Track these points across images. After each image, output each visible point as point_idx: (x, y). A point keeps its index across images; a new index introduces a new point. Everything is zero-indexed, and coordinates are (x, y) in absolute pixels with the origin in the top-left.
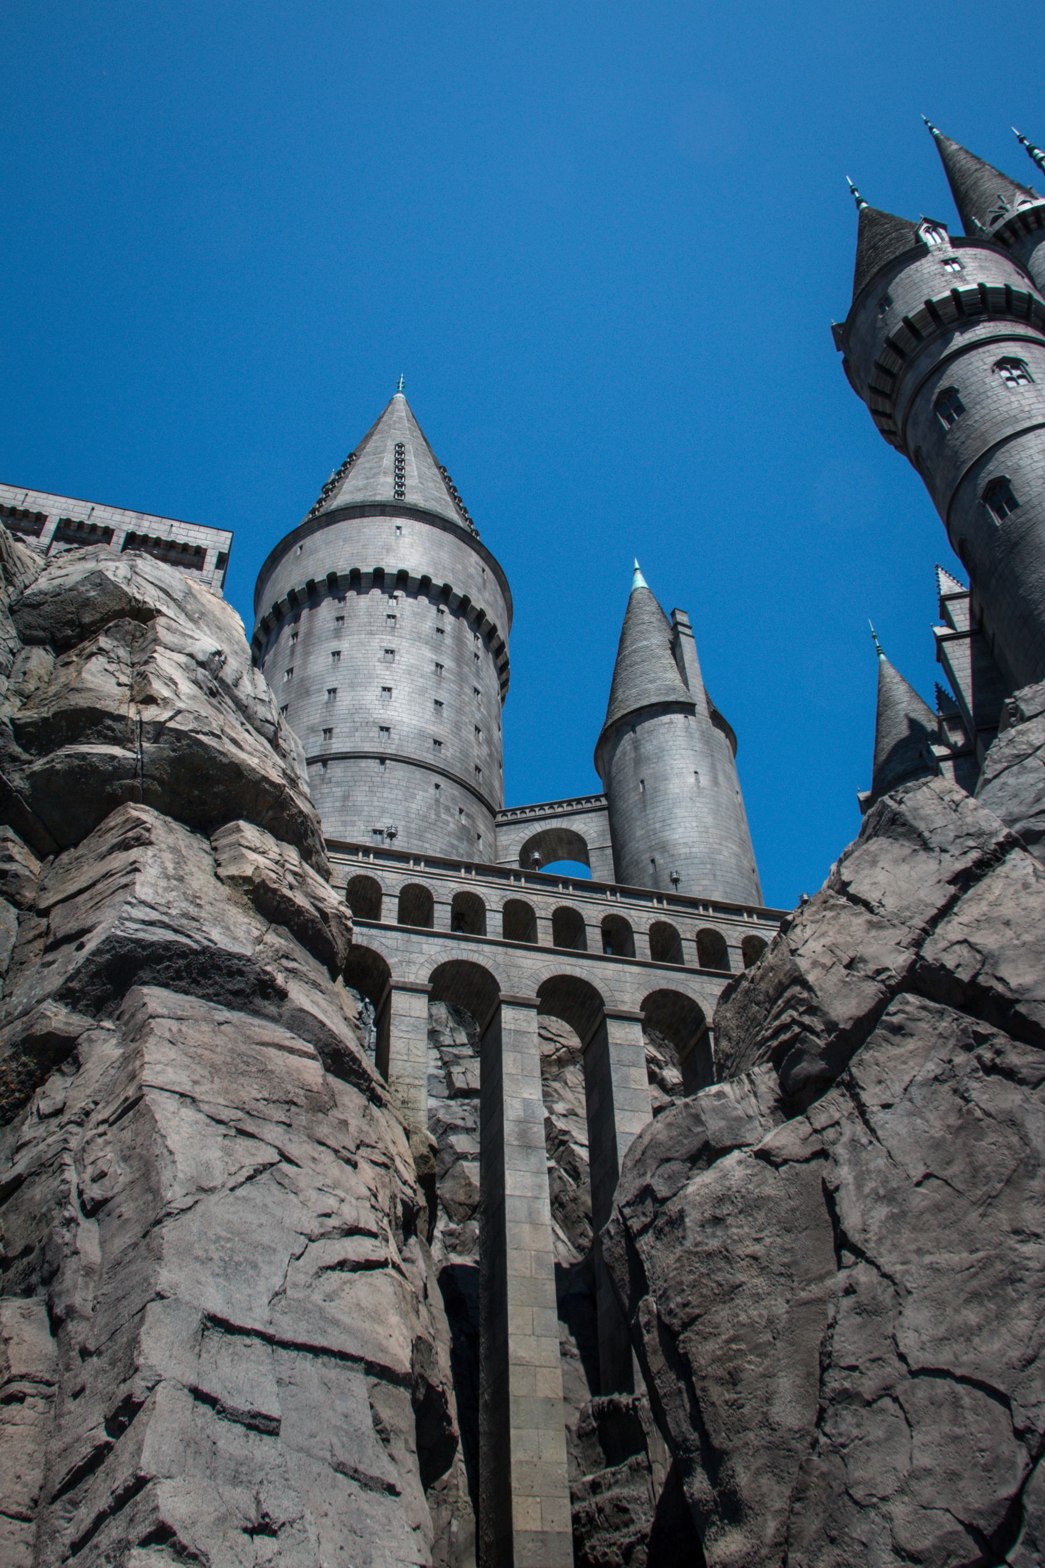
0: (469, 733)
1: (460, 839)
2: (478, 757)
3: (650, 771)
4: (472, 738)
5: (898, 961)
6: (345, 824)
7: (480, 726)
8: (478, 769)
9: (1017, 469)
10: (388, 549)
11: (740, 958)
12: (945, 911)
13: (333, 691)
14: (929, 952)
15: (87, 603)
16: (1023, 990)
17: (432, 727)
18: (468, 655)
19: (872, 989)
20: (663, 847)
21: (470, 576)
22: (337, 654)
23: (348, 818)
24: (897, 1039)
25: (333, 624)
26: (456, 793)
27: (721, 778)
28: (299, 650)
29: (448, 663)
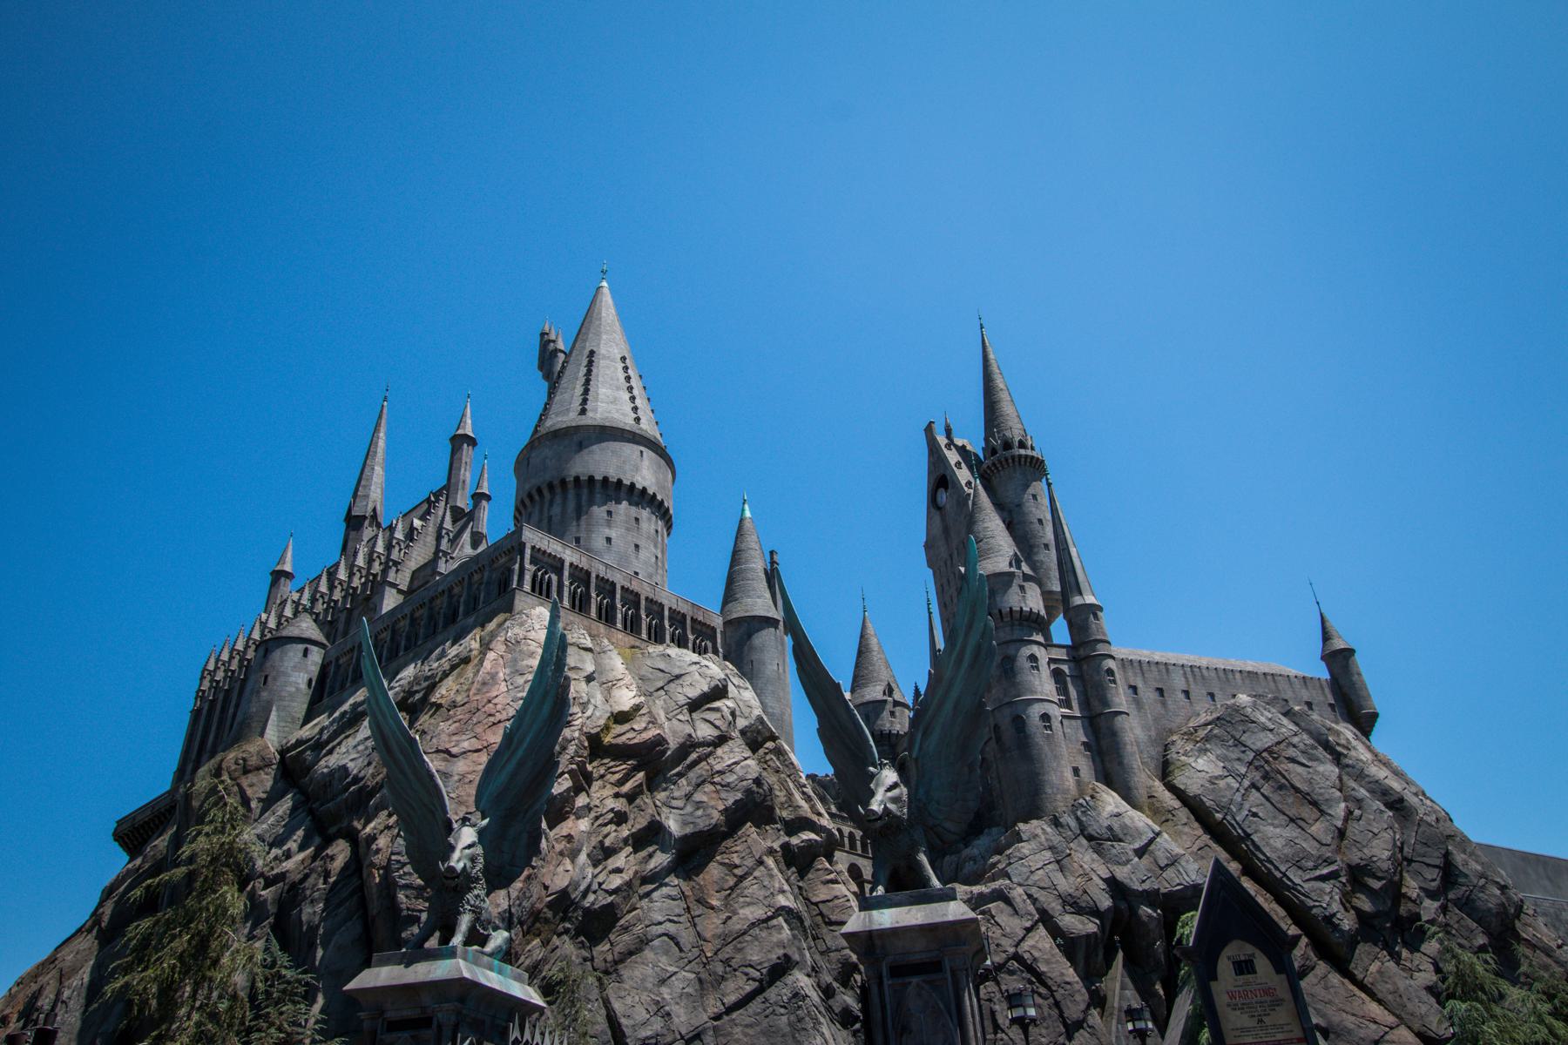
5: (1012, 950)
9: (1028, 717)
12: (1023, 939)
14: (1020, 951)
15: (759, 732)
19: (1004, 956)
22: (609, 540)
29: (659, 556)
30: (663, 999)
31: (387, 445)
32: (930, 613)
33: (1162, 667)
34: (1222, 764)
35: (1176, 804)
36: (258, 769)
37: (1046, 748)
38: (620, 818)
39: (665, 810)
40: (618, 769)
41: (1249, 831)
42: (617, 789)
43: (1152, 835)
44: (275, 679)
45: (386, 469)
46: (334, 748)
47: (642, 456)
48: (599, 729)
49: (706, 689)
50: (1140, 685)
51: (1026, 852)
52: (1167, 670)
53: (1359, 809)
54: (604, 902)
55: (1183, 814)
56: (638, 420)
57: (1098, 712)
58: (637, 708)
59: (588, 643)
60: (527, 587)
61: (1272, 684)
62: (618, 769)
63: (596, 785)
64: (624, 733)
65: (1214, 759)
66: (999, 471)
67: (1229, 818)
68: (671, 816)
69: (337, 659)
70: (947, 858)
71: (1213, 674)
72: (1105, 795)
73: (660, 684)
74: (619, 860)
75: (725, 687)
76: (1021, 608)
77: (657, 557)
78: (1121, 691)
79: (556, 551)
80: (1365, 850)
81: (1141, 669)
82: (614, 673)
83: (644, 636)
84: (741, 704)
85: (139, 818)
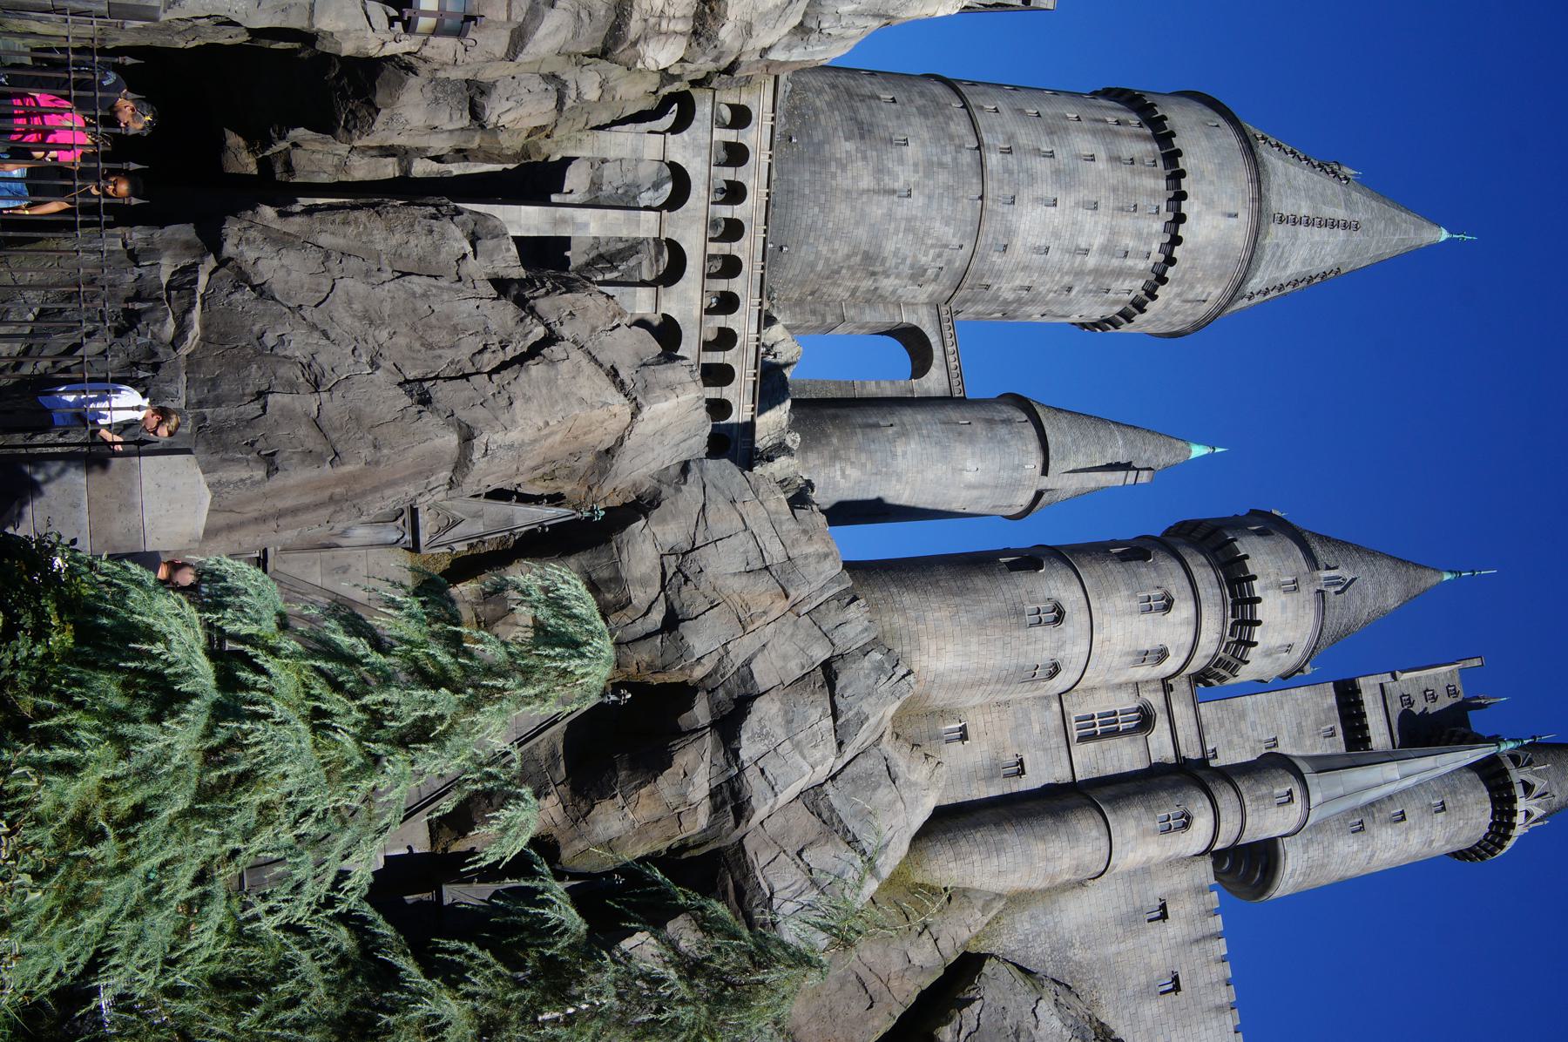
0: (1021, 279)
1: (912, 267)
2: (999, 288)
3: (979, 430)
4: (1017, 283)
6: (916, 165)
7: (1033, 292)
8: (988, 287)
10: (1209, 204)
11: (713, 396)
13: (1052, 155)
16: (527, 370)
17: (1019, 243)
18: (1107, 281)
20: (904, 434)
21: (1192, 287)
23: (921, 168)
24: (517, 319)
25: (1126, 155)
26: (957, 264)
27: (975, 493)
37: (996, 605)
43: (868, 841)
47: (1230, 216)
51: (772, 505)
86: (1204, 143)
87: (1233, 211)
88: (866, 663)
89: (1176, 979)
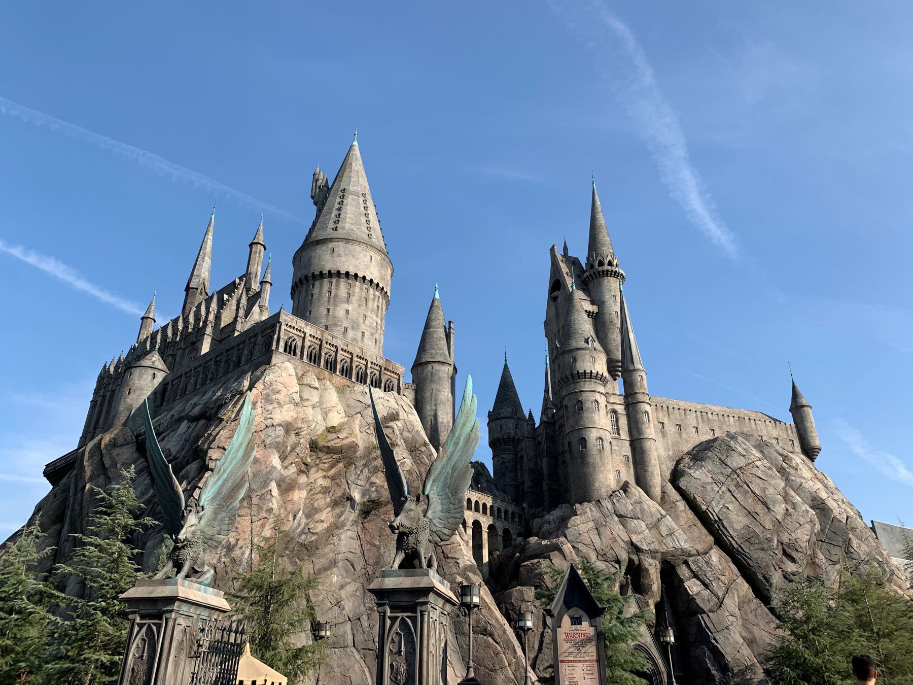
9: (589, 438)
28: (332, 300)
30: (341, 597)
31: (213, 242)
32: (546, 364)
33: (682, 411)
34: (710, 476)
35: (679, 498)
36: (122, 445)
37: (598, 458)
38: (325, 491)
39: (353, 486)
40: (326, 461)
41: (721, 518)
42: (325, 473)
44: (135, 391)
45: (212, 259)
46: (165, 437)
48: (317, 437)
49: (385, 414)
50: (666, 422)
51: (579, 522)
52: (685, 414)
53: (793, 509)
54: (311, 540)
55: (682, 505)
56: (370, 236)
57: (636, 438)
58: (342, 425)
59: (316, 384)
60: (281, 349)
61: (753, 426)
62: (326, 461)
63: (313, 470)
64: (333, 440)
65: (706, 472)
66: (593, 279)
67: (710, 509)
68: (357, 490)
69: (172, 381)
70: (536, 520)
71: (715, 417)
72: (633, 489)
73: (359, 410)
74: (323, 515)
75: (398, 414)
76: (591, 371)
77: (377, 323)
78: (652, 425)
79: (301, 327)
80: (793, 535)
81: (668, 412)
82: (331, 403)
83: (354, 379)
84: (407, 423)
85: (58, 464)
86: (343, 259)
87: (370, 257)
88: (617, 504)
89: (677, 425)
